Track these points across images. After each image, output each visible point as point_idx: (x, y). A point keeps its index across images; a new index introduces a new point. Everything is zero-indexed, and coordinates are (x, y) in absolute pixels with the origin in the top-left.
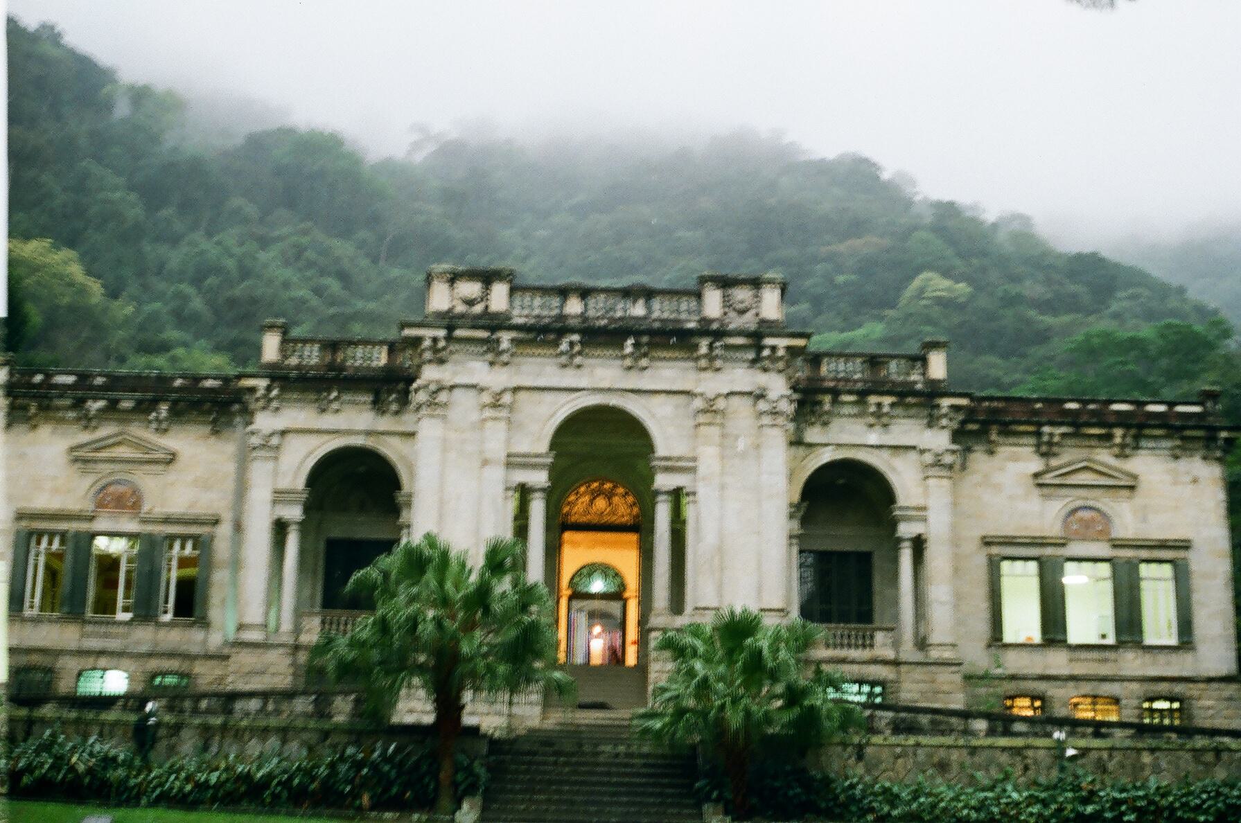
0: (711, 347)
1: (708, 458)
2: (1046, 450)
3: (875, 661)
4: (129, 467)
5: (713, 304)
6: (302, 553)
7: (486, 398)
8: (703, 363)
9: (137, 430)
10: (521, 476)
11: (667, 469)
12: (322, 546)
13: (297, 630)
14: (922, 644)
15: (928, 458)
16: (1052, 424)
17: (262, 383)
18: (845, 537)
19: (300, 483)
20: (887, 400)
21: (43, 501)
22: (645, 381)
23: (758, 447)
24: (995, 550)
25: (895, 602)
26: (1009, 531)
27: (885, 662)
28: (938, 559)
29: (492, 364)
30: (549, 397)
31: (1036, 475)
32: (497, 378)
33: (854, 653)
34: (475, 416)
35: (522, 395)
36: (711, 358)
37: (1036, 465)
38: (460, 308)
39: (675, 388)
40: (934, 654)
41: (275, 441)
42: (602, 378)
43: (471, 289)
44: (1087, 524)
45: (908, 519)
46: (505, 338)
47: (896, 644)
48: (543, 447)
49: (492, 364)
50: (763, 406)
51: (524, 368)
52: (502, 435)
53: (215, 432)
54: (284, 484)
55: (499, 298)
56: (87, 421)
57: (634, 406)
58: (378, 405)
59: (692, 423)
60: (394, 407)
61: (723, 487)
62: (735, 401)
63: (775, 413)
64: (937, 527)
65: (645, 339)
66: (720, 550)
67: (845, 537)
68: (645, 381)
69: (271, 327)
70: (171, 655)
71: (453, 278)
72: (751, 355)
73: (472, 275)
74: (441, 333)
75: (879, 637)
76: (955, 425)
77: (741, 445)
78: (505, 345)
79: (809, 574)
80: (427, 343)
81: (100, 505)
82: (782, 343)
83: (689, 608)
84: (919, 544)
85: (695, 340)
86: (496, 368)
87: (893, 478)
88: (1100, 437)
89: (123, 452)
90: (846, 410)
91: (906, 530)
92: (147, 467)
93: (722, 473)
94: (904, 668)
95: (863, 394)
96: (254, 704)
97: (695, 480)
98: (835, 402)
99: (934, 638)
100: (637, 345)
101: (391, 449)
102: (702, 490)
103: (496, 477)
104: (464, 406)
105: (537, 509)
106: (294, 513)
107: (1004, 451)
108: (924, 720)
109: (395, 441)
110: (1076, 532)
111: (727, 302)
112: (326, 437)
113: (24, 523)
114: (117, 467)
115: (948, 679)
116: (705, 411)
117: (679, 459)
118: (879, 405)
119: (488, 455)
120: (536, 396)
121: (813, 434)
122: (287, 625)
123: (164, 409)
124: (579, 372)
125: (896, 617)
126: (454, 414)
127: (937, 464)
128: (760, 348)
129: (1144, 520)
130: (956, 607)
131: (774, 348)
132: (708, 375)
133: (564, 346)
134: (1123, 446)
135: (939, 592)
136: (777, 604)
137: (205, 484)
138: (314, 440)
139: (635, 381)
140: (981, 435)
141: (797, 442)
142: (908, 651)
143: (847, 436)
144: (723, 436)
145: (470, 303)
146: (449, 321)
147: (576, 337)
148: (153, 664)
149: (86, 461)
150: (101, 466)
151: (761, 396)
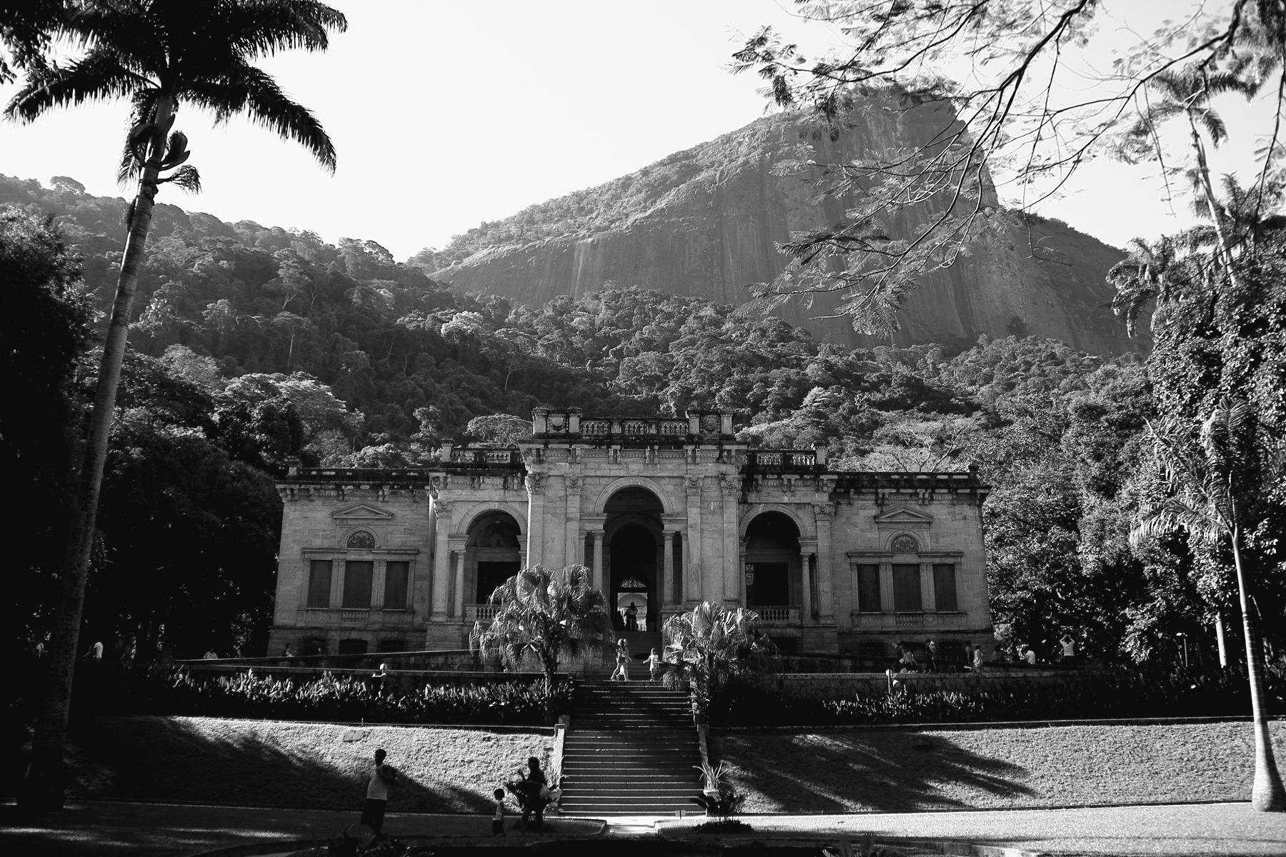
0: (694, 451)
1: (694, 514)
2: (880, 502)
3: (789, 626)
5: (695, 427)
6: (465, 570)
7: (568, 483)
8: (690, 460)
9: (370, 500)
11: (670, 521)
12: (476, 566)
13: (464, 615)
14: (815, 615)
15: (817, 510)
16: (884, 487)
17: (441, 475)
18: (768, 555)
19: (464, 530)
20: (794, 477)
21: (317, 543)
23: (721, 508)
24: (854, 560)
25: (801, 591)
26: (862, 548)
27: (796, 627)
28: (824, 568)
29: (571, 463)
30: (603, 481)
31: (875, 517)
33: (778, 622)
34: (562, 493)
35: (588, 481)
36: (694, 458)
37: (874, 511)
38: (552, 431)
40: (822, 621)
41: (449, 508)
42: (631, 470)
43: (557, 420)
44: (905, 544)
45: (807, 545)
46: (579, 449)
47: (801, 616)
50: (723, 484)
51: (589, 465)
52: (577, 504)
53: (415, 502)
54: (454, 531)
55: (574, 424)
56: (341, 496)
57: (652, 486)
58: (505, 488)
59: (683, 495)
61: (702, 531)
62: (708, 481)
63: (731, 487)
64: (823, 545)
65: (656, 447)
66: (701, 566)
67: (768, 555)
69: (447, 442)
70: (393, 629)
71: (547, 415)
73: (558, 412)
75: (792, 612)
76: (830, 490)
79: (751, 576)
80: (534, 452)
81: (351, 545)
82: (734, 448)
83: (684, 600)
84: (813, 559)
87: (797, 522)
88: (911, 495)
90: (770, 483)
91: (806, 551)
94: (805, 630)
95: (779, 475)
96: (441, 660)
98: (764, 478)
99: (823, 612)
100: (652, 450)
101: (513, 509)
102: (690, 532)
103: (574, 526)
104: (555, 488)
105: (598, 544)
106: (460, 547)
107: (858, 503)
108: (817, 661)
110: (899, 550)
111: (702, 424)
113: (307, 556)
115: (829, 634)
117: (678, 515)
118: (789, 480)
121: (752, 497)
122: (458, 612)
123: (387, 490)
125: (801, 601)
126: (549, 493)
127: (822, 512)
128: (721, 452)
129: (937, 541)
130: (833, 594)
131: (729, 451)
133: (611, 453)
134: (924, 499)
135: (824, 586)
136: (733, 596)
137: (410, 532)
138: (470, 506)
140: (846, 494)
141: (743, 501)
142: (808, 621)
143: (773, 498)
145: (557, 428)
146: (545, 438)
147: (618, 447)
148: (383, 635)
151: (724, 479)
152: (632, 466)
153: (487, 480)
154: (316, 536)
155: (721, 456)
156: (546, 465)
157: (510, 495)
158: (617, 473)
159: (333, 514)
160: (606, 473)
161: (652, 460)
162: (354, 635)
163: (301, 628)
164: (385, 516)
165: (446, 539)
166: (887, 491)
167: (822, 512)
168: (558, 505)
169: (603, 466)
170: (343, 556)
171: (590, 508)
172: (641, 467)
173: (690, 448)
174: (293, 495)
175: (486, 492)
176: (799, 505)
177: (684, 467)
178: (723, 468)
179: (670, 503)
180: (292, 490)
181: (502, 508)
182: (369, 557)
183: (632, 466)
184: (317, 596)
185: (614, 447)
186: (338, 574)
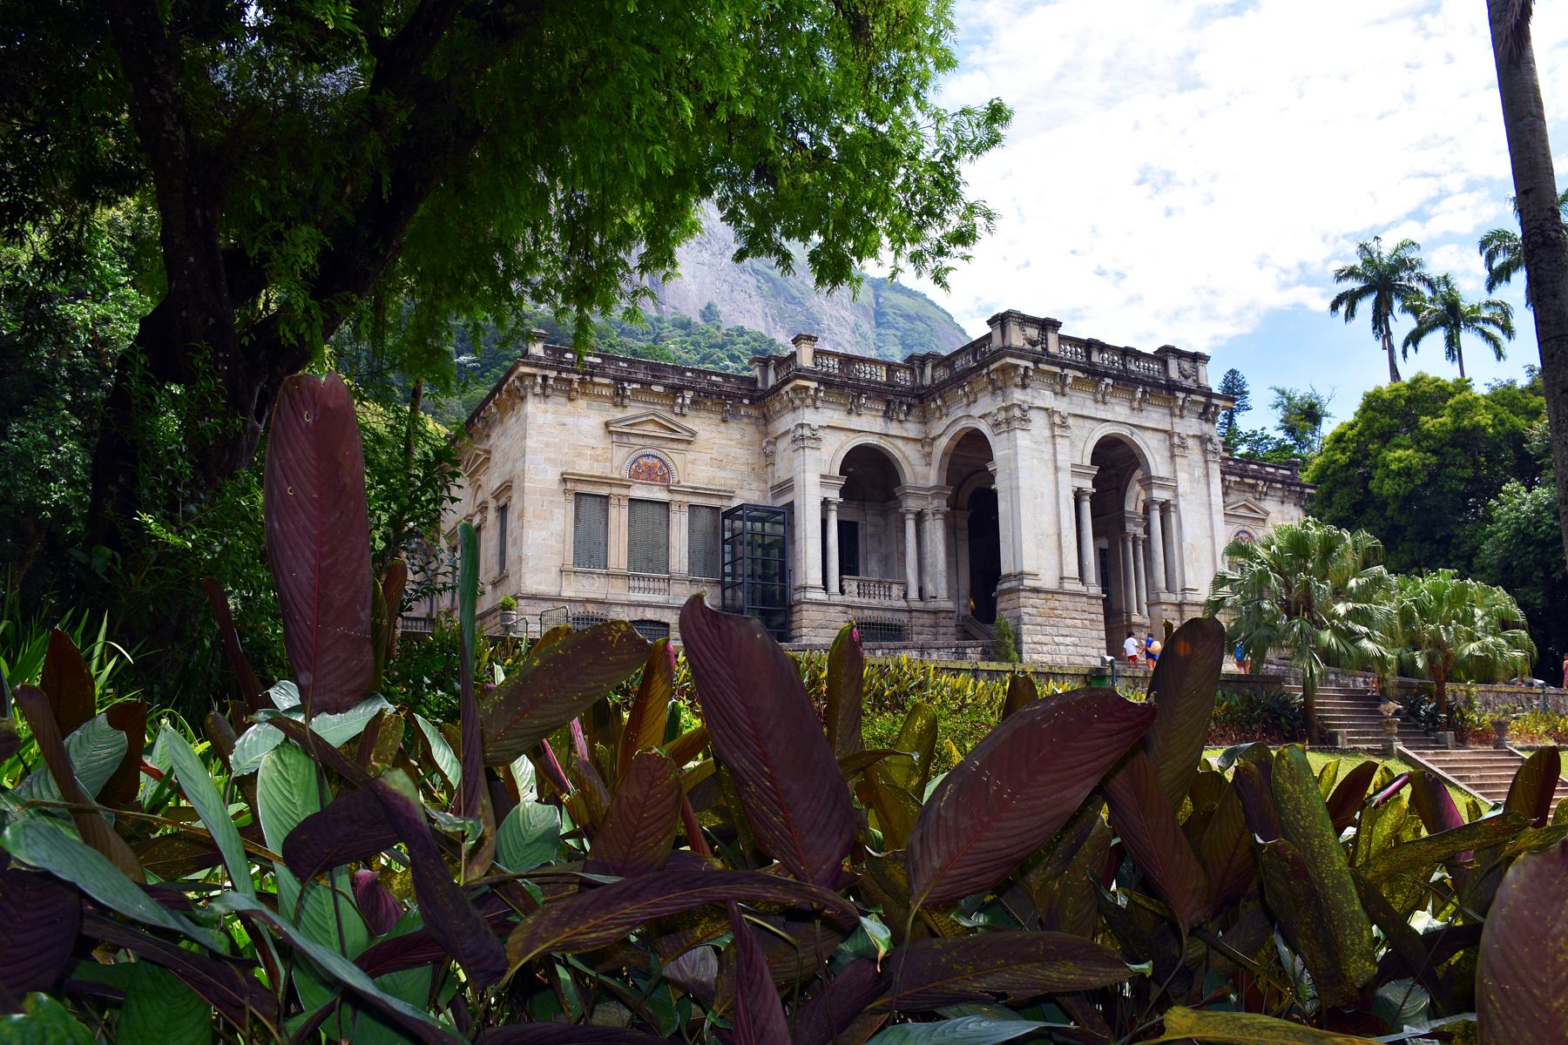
4: (657, 442)
11: (1161, 487)
17: (813, 385)
21: (584, 467)
30: (1088, 423)
32: (1061, 405)
34: (1047, 433)
36: (1182, 408)
42: (1118, 415)
43: (1033, 333)
46: (1070, 373)
48: (1087, 462)
50: (1210, 447)
53: (724, 421)
56: (619, 398)
58: (887, 416)
60: (902, 417)
74: (1031, 365)
78: (1069, 380)
89: (650, 429)
92: (675, 445)
97: (1176, 496)
100: (1144, 392)
102: (1182, 504)
104: (1039, 421)
105: (1086, 506)
109: (900, 443)
112: (852, 435)
113: (569, 486)
114: (648, 442)
123: (689, 395)
132: (1176, 420)
138: (842, 436)
145: (1033, 343)
147: (1110, 381)
149: (621, 434)
150: (633, 440)
152: (1118, 409)
154: (580, 455)
156: (1029, 390)
157: (894, 429)
159: (607, 424)
162: (650, 615)
163: (570, 601)
164: (684, 435)
165: (819, 480)
166: (1233, 478)
168: (1043, 447)
169: (1090, 403)
170: (624, 492)
173: (1181, 395)
174: (544, 386)
175: (864, 418)
177: (1168, 419)
178: (1207, 428)
179: (1158, 463)
180: (545, 378)
181: (883, 443)
182: (660, 495)
184: (588, 552)
186: (619, 517)
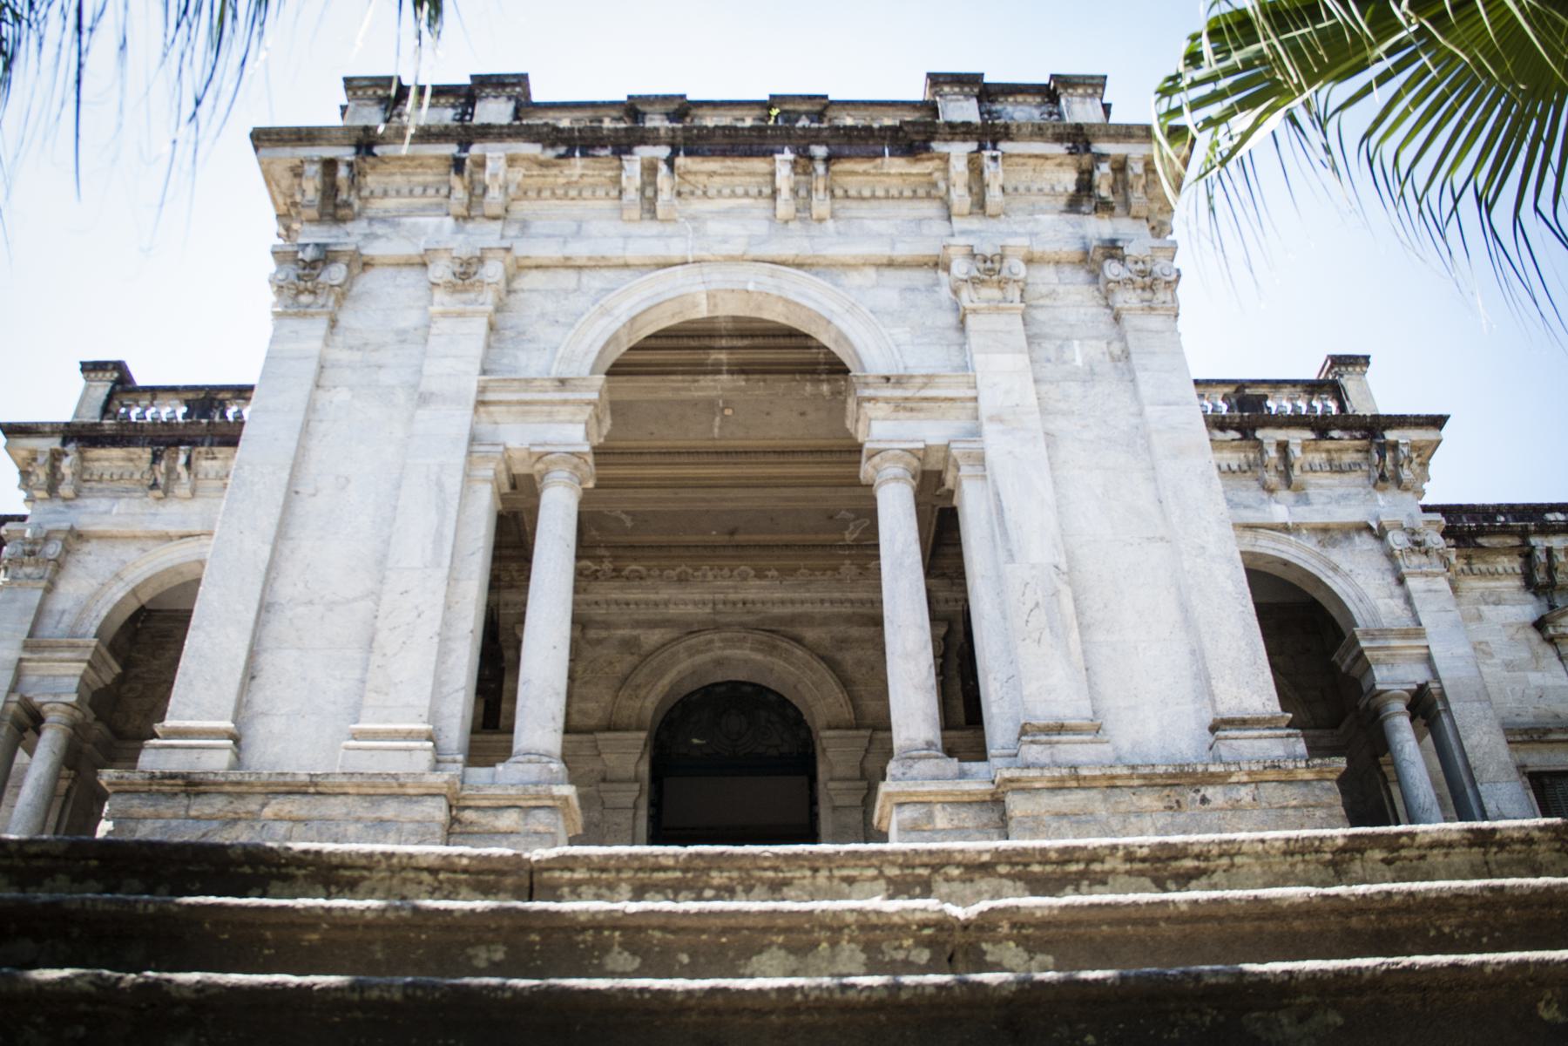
0: (976, 169)
1: (1001, 370)
8: (960, 197)
10: (518, 436)
15: (1397, 540)
22: (830, 243)
30: (593, 281)
34: (412, 319)
39: (903, 251)
45: (1392, 656)
49: (467, 218)
50: (1112, 269)
51: (538, 227)
65: (820, 151)
68: (830, 243)
72: (1068, 180)
74: (346, 153)
77: (1078, 355)
80: (313, 170)
85: (938, 146)
86: (470, 226)
93: (1044, 411)
97: (976, 433)
100: (804, 160)
116: (976, 282)
118: (1283, 447)
119: (428, 385)
120: (568, 279)
124: (670, 228)
138: (131, 552)
139: (794, 244)
144: (1031, 339)
147: (663, 151)
152: (714, 227)
153: (205, 465)
155: (1085, 185)
156: (357, 229)
158: (658, 250)
160: (612, 248)
161: (803, 196)
167: (1418, 546)
171: (532, 362)
172: (761, 228)
175: (197, 506)
176: (1327, 534)
177: (940, 227)
183: (714, 227)
185: (644, 152)
